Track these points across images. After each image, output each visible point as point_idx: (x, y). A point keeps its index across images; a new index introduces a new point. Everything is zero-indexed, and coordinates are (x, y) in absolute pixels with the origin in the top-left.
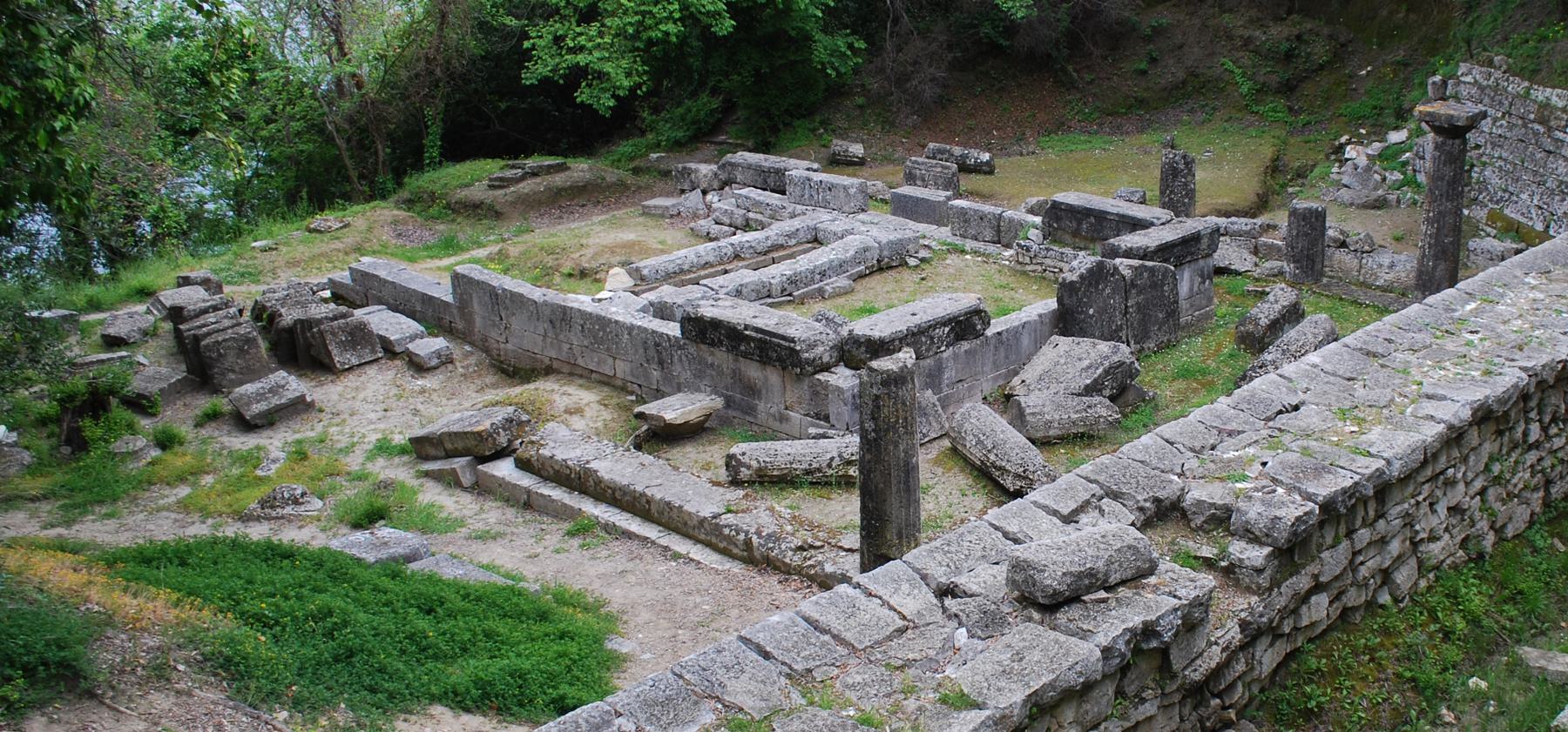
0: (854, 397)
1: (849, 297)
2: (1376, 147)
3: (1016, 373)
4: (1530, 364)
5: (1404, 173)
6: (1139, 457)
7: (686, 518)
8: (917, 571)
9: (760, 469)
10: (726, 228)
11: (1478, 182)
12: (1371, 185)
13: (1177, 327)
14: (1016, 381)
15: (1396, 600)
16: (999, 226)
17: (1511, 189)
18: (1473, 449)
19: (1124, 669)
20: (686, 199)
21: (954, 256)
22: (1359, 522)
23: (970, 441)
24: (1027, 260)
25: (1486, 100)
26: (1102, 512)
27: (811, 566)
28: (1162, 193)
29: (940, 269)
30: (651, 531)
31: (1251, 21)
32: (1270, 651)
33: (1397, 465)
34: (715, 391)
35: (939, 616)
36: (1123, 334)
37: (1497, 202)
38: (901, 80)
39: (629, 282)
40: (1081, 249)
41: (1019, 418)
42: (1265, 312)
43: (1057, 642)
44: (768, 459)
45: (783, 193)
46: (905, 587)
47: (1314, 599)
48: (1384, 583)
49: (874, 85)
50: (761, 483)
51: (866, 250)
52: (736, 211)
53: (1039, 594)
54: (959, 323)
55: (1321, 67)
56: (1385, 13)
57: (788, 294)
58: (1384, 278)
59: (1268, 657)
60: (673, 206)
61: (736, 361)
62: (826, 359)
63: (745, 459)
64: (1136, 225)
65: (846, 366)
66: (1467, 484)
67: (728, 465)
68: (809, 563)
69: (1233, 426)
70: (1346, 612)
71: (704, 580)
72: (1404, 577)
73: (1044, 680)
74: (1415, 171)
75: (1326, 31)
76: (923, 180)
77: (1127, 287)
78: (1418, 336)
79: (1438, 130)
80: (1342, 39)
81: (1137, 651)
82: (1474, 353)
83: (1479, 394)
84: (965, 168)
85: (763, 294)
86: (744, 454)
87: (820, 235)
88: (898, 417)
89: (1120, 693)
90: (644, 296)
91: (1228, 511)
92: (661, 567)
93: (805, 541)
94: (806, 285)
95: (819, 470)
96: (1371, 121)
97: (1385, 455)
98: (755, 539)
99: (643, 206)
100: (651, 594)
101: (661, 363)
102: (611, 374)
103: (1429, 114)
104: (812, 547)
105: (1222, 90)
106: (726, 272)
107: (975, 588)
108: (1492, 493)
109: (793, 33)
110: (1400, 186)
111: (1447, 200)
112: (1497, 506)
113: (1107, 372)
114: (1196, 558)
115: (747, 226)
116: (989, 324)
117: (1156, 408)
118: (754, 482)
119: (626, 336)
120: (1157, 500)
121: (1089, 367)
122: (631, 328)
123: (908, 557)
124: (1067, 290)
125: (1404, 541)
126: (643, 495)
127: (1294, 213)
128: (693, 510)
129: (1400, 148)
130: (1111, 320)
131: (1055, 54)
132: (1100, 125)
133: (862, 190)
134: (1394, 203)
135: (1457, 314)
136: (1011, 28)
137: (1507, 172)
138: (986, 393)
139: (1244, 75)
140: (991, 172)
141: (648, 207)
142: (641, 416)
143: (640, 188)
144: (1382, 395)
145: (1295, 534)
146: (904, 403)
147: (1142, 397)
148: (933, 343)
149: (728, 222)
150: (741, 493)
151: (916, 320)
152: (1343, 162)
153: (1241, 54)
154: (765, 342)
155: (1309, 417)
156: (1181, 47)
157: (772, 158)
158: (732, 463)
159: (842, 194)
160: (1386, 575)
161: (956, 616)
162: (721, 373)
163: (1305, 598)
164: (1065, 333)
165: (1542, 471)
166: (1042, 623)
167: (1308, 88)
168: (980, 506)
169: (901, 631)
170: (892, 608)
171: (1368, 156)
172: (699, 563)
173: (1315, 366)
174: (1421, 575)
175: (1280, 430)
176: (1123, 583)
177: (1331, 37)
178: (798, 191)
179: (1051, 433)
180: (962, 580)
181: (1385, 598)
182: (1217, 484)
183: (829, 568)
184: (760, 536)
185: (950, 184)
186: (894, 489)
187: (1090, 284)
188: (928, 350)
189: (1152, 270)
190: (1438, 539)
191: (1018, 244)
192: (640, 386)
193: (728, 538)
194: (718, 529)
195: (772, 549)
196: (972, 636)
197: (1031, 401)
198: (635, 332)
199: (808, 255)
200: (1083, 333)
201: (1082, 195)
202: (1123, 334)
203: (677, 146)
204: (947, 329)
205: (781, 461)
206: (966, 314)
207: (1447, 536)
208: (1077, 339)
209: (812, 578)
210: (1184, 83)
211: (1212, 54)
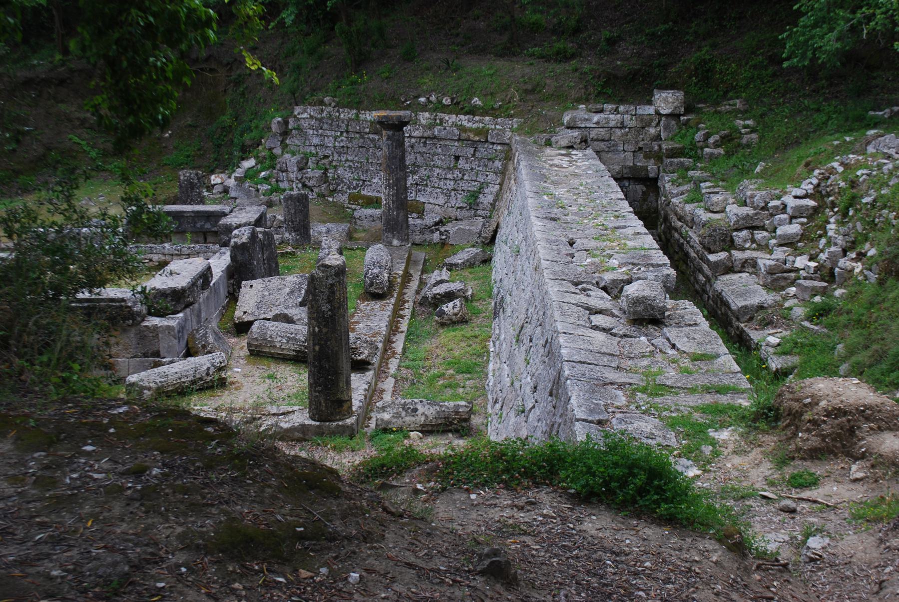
9: (158, 388)
11: (334, 179)
25: (325, 126)
27: (266, 430)
37: (355, 188)
44: (163, 380)
74: (277, 181)
95: (201, 379)
111: (401, 170)
121: (292, 292)
134: (278, 203)
137: (356, 168)
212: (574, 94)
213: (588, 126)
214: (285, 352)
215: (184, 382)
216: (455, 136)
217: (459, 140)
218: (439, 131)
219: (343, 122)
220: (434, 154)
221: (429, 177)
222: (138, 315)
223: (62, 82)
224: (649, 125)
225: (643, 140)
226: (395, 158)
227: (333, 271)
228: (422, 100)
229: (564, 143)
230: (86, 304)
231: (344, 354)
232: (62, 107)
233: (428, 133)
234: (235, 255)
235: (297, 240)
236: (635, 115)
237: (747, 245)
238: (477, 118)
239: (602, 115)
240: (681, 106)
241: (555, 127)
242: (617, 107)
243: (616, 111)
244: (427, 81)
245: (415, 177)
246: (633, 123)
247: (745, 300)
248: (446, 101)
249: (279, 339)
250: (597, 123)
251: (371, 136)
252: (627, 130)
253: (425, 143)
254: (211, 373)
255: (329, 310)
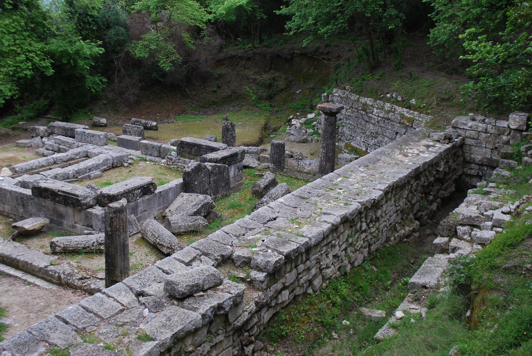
0: (102, 218)
1: (100, 179)
2: (303, 119)
3: (167, 207)
4: (362, 201)
5: (314, 130)
6: (215, 239)
7: (34, 268)
8: (128, 286)
9: (64, 247)
10: (51, 152)
11: (341, 133)
12: (302, 134)
13: (229, 189)
14: (167, 210)
15: (314, 292)
16: (160, 150)
17: (353, 135)
18: (342, 233)
19: (211, 323)
20: (34, 140)
21: (142, 162)
22: (299, 262)
23: (149, 234)
24: (171, 163)
25: (343, 102)
26: (201, 261)
28: (223, 137)
29: (137, 167)
30: (19, 274)
31: (256, 73)
32: (267, 313)
33: (313, 240)
34: (46, 216)
35: (137, 304)
36: (209, 192)
37: (348, 140)
38: (121, 94)
39: (10, 173)
40: (192, 159)
41: (168, 225)
42: (262, 183)
43: (184, 313)
44: (68, 243)
45: (74, 138)
46: (123, 293)
47: (283, 292)
48: (310, 285)
49: (110, 95)
50: (65, 253)
51: (107, 160)
52: (55, 145)
53: (177, 294)
54: (144, 188)
55: (282, 90)
56: (306, 70)
57: (76, 178)
58: (307, 169)
59: (266, 316)
60: (29, 143)
61: (55, 204)
62: (91, 203)
63: (58, 244)
64: (213, 150)
65: (100, 206)
66: (340, 246)
67: (51, 246)
68: (84, 284)
69: (251, 226)
70: (295, 297)
71: (41, 293)
72: (317, 282)
73: (179, 328)
74: (318, 129)
75: (284, 76)
76: (130, 133)
77: (210, 174)
78: (320, 191)
79: (326, 113)
80: (290, 80)
81: (216, 315)
82: (341, 197)
83: (343, 212)
84: (146, 128)
85: (66, 178)
86: (58, 241)
87: (89, 154)
88: (120, 226)
89: (209, 332)
90: (17, 179)
91: (250, 259)
92: (23, 288)
93: (83, 276)
94: (83, 174)
95: (88, 247)
96: (301, 110)
97: (309, 236)
98: (62, 276)
99: (17, 143)
100: (18, 299)
101: (23, 206)
102: (2, 210)
103: (322, 107)
104: (86, 278)
105: (245, 98)
106: (50, 169)
107: (151, 293)
108: (349, 250)
109: (78, 75)
110: (312, 134)
111: (330, 139)
112: (351, 254)
113: (202, 206)
114: (238, 278)
115: (59, 151)
116: (156, 188)
117: (222, 220)
118: (62, 253)
119: (9, 195)
120: (222, 256)
121: (195, 205)
122: (11, 192)
123: (124, 281)
124: (186, 175)
125: (317, 269)
126: (15, 259)
127: (273, 145)
128: (36, 265)
129: (312, 120)
130: (204, 187)
131: (181, 84)
132: (199, 112)
133: (106, 136)
134: (310, 141)
135: (334, 182)
136: (164, 74)
138: (155, 215)
139: (253, 93)
140: (157, 130)
141: (18, 143)
142: (15, 227)
143: (15, 135)
144: (307, 213)
145: (275, 267)
146: (123, 220)
147: (216, 216)
148: (134, 196)
149: (51, 149)
150: (56, 257)
151: (127, 187)
152: (291, 125)
153: (252, 85)
154: (66, 197)
155: (280, 222)
156: (229, 82)
157: (69, 124)
158: (53, 245)
159: (98, 138)
160: (310, 282)
161: (144, 304)
162: (48, 209)
163: (280, 292)
164: (186, 192)
165: (367, 241)
166: (178, 305)
167: (277, 98)
168: (153, 260)
169: (122, 311)
170: (118, 302)
171: (300, 123)
172: (39, 286)
173: (282, 203)
174: (323, 282)
175: (269, 227)
176: (210, 288)
177: (285, 79)
178: (80, 137)
179: (181, 230)
180: (146, 290)
181: (310, 291)
182: (245, 249)
183: (93, 286)
184: (64, 274)
185: (141, 134)
186: (119, 254)
187: (196, 173)
188: (132, 199)
189: (219, 167)
190: (330, 268)
191: (167, 157)
192: (15, 215)
193: (51, 276)
194: (47, 272)
195: (69, 279)
196: (150, 312)
197: (173, 218)
198: (13, 193)
199: (84, 162)
200: (193, 191)
201: (192, 138)
202: (209, 192)
203: (30, 119)
204: (140, 191)
205: (73, 244)
206: (147, 184)
207: (333, 267)
208: (191, 194)
209: (86, 291)
210: (231, 96)
211: (241, 85)
212: (469, 106)
213: (465, 128)
214: (150, 241)
215: (79, 247)
216: (398, 120)
217: (400, 123)
218: (391, 116)
219: (351, 102)
220: (388, 129)
221: (381, 142)
222: (84, 205)
223: (249, 59)
224: (503, 134)
225: (498, 143)
226: (328, 132)
227: (113, 210)
228: (388, 95)
229: (436, 138)
230: (64, 194)
231: (119, 256)
232: (246, 71)
233: (386, 116)
234: (185, 177)
235: (274, 168)
236: (495, 126)
237: (465, 237)
238: (411, 112)
239: (474, 123)
240: (524, 125)
241: (446, 126)
242: (485, 119)
243: (483, 121)
244: (396, 85)
245: (376, 140)
246: (493, 131)
247: (419, 278)
248: (399, 99)
249: (150, 233)
250: (471, 127)
251: (362, 112)
252: (489, 134)
253: (384, 121)
254: (95, 245)
255: (110, 231)
